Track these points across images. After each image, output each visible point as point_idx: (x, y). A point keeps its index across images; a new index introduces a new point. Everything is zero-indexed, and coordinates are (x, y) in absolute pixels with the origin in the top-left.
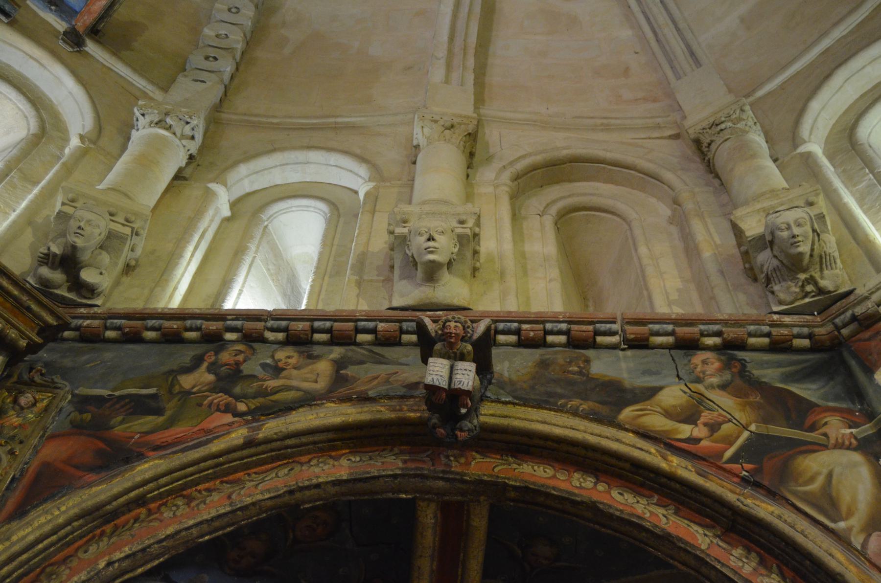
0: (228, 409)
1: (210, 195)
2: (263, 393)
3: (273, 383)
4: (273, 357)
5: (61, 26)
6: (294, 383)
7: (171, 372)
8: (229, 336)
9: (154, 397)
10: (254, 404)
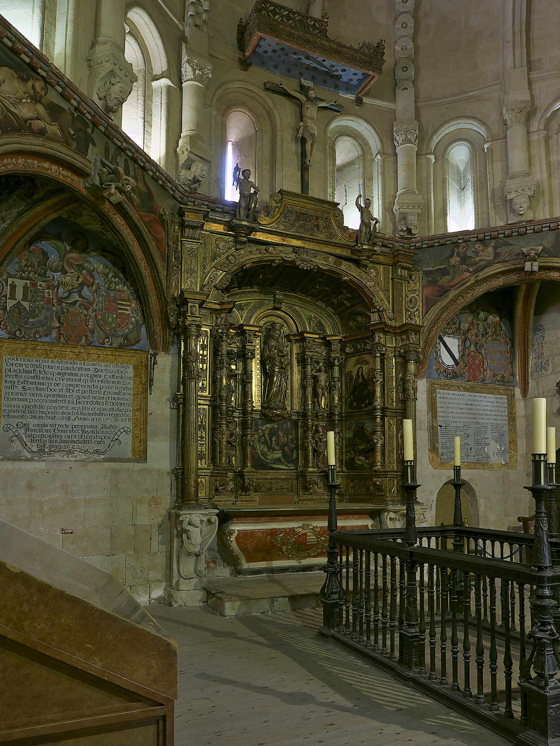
0: (468, 271)
2: (475, 263)
3: (477, 259)
4: (474, 247)
5: (352, 97)
6: (483, 258)
7: (447, 258)
8: (459, 241)
9: (445, 268)
10: (474, 268)
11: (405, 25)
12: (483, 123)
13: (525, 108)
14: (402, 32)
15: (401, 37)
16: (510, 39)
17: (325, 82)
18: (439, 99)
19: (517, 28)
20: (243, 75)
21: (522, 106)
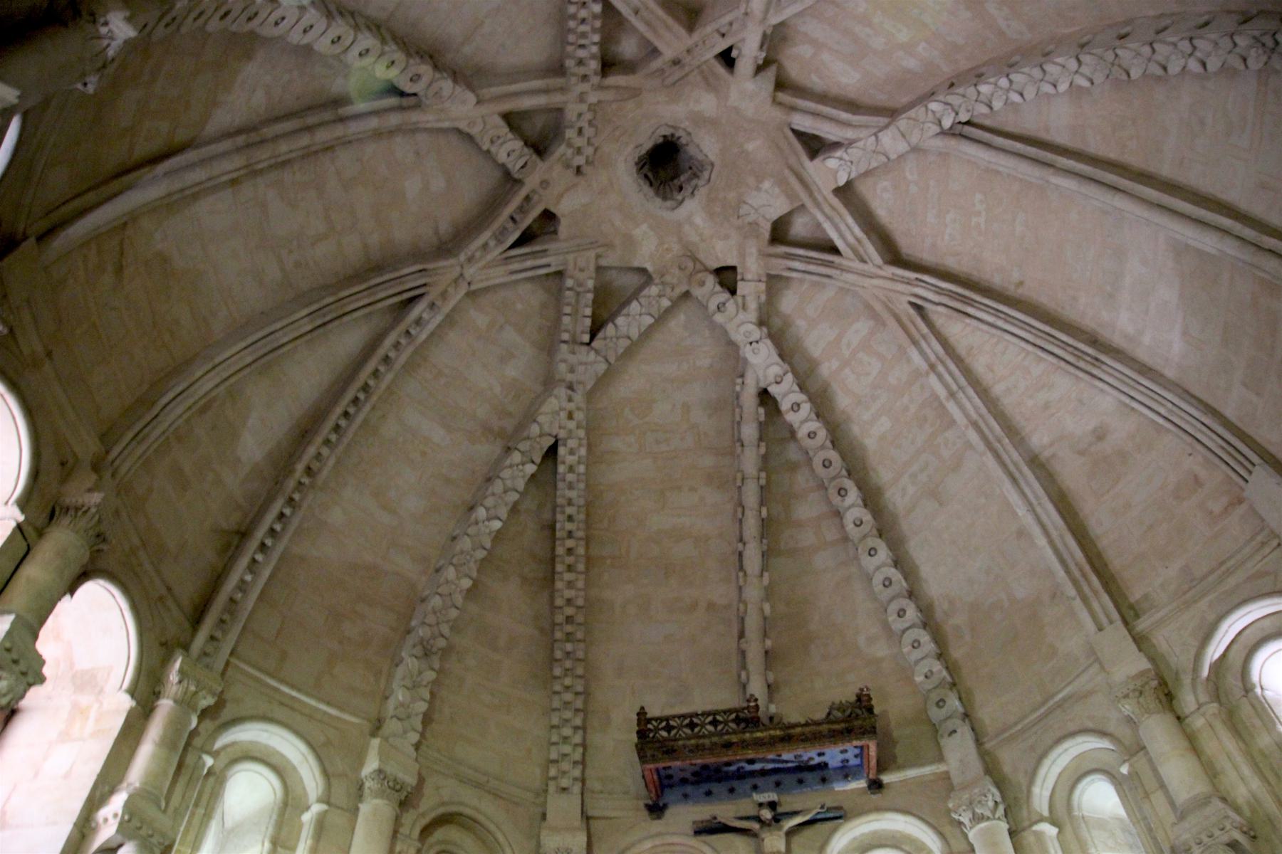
1: (1039, 835)
11: (916, 644)
12: (1103, 734)
13: (1147, 683)
14: (916, 654)
15: (917, 662)
16: (1072, 592)
17: (801, 781)
18: (1016, 724)
19: (1077, 574)
20: (656, 826)
21: (1139, 683)
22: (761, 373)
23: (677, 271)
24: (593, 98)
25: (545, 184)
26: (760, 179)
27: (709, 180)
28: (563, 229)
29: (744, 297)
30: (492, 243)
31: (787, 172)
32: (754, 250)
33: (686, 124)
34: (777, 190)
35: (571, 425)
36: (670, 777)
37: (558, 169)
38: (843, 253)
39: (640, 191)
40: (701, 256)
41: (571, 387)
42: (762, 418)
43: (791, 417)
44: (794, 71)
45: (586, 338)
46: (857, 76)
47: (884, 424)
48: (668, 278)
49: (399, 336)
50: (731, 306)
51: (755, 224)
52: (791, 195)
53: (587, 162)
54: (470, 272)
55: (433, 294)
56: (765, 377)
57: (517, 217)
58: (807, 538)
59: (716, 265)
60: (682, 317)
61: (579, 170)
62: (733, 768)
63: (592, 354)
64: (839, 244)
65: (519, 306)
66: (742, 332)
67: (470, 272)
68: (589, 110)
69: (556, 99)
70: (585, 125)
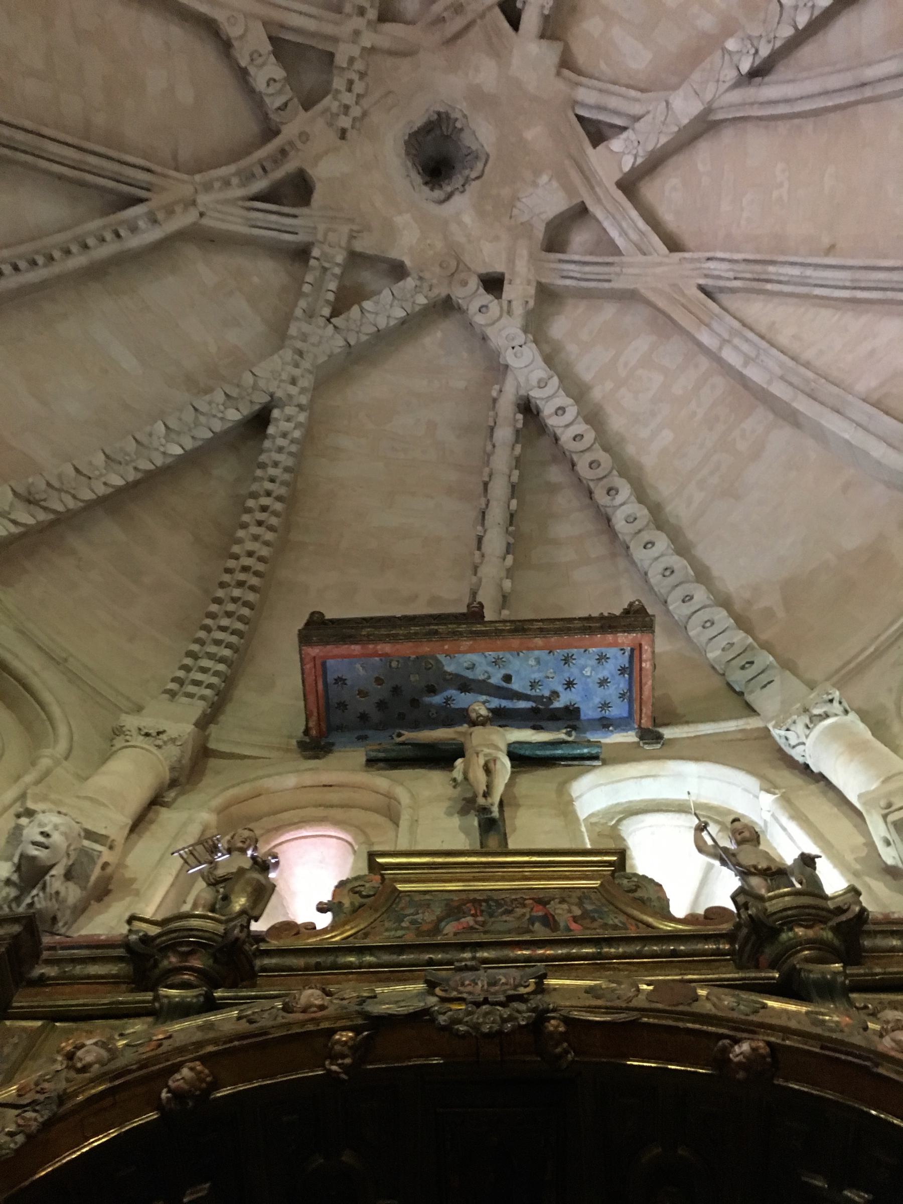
22: (522, 380)
23: (437, 270)
24: (369, 38)
25: (304, 137)
26: (537, 173)
27: (483, 171)
28: (317, 197)
29: (510, 302)
30: (235, 181)
31: (567, 162)
32: (525, 253)
33: (463, 106)
34: (555, 184)
35: (293, 390)
36: (342, 706)
37: (320, 123)
38: (624, 252)
39: (408, 176)
40: (466, 258)
41: (300, 353)
42: (520, 425)
43: (553, 422)
44: (581, 56)
45: (327, 312)
46: (648, 56)
47: (667, 436)
48: (427, 275)
49: (104, 227)
50: (494, 306)
51: (527, 227)
52: (569, 189)
53: (353, 127)
54: (203, 199)
55: (157, 201)
56: (527, 380)
57: (268, 165)
58: (567, 555)
59: (483, 270)
60: (439, 334)
61: (343, 135)
62: (437, 699)
63: (331, 327)
64: (620, 242)
65: (256, 280)
66: (504, 336)
67: (203, 199)
68: (361, 56)
69: (329, 29)
70: (355, 77)
